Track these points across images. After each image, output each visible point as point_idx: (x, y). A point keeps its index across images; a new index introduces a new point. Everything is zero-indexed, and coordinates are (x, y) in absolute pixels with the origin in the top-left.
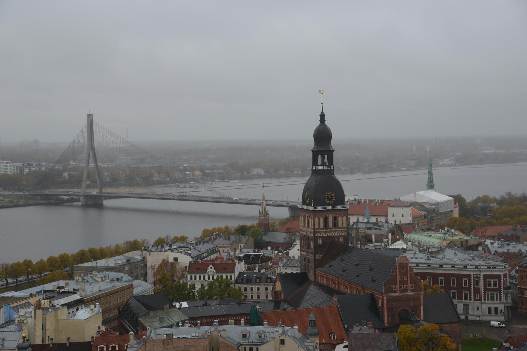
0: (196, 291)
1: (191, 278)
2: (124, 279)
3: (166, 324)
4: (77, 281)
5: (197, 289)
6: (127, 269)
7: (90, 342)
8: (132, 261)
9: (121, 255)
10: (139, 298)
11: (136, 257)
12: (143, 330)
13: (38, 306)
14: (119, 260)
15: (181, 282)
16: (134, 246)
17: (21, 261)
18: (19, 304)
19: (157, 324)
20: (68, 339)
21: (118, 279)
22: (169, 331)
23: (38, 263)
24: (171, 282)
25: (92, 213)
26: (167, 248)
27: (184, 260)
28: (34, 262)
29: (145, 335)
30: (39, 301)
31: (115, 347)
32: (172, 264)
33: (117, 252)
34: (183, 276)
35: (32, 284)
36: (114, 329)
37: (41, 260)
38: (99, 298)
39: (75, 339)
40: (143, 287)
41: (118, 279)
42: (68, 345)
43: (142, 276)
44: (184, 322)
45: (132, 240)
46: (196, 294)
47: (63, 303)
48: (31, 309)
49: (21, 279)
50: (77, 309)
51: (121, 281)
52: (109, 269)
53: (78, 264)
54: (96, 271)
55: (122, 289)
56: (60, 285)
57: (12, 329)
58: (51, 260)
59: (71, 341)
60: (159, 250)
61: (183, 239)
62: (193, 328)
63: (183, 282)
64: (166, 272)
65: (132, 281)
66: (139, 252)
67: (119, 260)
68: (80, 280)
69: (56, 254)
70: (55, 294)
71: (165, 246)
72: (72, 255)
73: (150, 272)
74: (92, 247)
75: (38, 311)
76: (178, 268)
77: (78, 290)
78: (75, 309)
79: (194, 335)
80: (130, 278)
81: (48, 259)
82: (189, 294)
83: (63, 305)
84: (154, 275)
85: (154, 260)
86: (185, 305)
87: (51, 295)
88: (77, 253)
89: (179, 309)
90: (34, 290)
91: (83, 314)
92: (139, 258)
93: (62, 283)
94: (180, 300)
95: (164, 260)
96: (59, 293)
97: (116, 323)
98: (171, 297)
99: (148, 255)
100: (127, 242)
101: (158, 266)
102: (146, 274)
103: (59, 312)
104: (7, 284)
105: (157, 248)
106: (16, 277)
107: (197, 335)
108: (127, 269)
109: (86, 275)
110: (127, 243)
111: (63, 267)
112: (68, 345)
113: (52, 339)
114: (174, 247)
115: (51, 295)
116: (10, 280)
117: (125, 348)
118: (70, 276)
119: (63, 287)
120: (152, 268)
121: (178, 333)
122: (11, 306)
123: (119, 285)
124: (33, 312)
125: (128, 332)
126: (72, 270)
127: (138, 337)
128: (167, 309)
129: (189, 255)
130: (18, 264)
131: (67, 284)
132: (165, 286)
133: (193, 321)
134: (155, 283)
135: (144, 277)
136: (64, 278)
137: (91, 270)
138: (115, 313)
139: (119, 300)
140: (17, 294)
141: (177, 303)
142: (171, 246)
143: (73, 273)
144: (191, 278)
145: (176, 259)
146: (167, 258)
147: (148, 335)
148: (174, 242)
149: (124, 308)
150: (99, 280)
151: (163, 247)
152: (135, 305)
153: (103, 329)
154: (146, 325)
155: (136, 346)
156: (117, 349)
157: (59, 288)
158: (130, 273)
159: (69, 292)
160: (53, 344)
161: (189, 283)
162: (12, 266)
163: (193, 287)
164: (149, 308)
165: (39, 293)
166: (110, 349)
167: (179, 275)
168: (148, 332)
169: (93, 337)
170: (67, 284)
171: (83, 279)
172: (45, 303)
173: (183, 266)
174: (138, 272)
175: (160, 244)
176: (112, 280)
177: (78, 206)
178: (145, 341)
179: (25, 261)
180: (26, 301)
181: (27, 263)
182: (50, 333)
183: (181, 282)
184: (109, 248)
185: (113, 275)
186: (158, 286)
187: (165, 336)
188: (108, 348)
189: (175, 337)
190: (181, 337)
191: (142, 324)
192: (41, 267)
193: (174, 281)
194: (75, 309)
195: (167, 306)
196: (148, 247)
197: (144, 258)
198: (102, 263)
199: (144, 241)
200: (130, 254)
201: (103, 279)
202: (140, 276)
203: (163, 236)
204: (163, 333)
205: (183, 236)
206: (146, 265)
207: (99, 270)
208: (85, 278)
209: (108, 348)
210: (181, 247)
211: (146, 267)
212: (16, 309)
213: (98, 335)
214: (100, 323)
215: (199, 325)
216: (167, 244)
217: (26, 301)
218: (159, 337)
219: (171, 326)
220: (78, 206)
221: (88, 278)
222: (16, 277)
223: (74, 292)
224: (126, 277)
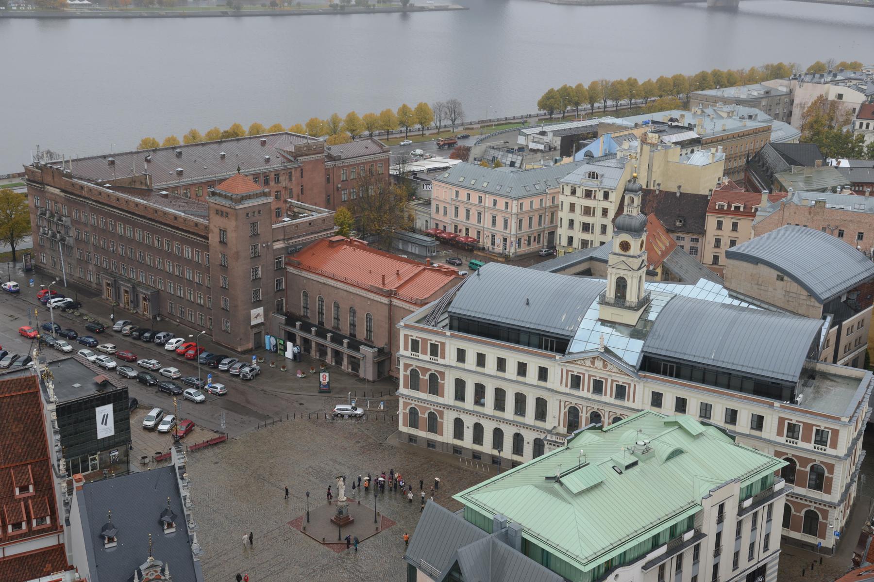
0: (866, 143)
1: (861, 126)
2: (759, 118)
3: (815, 187)
4: (695, 113)
5: (866, 143)
6: (764, 103)
7: (707, 196)
8: (773, 93)
9: (757, 82)
10: (776, 146)
11: (780, 88)
12: (780, 190)
13: (644, 141)
14: (756, 90)
15: (845, 130)
16: (777, 72)
17: (625, 79)
18: (622, 134)
19: (801, 185)
20: (679, 187)
21: (750, 117)
22: (821, 196)
23: (644, 84)
24: (826, 128)
25: (721, 18)
26: (829, 79)
27: (854, 98)
28: (640, 82)
29: (784, 197)
30: (645, 134)
31: (739, 207)
32: (833, 104)
33: (750, 79)
34: (847, 122)
35: (635, 111)
36: (738, 183)
37: (649, 80)
38: (722, 140)
39: (688, 189)
40: (785, 132)
41: (750, 117)
42: (678, 195)
43: (784, 116)
44: (843, 188)
45: (775, 63)
46: (865, 150)
47: (675, 140)
48: (636, 143)
49: (622, 102)
50: (692, 152)
51: (755, 120)
52: (739, 102)
53: (696, 90)
54: (721, 103)
55: (756, 132)
56: (674, 117)
57: (613, 165)
58: (662, 81)
59: (683, 190)
60: (815, 80)
61: (855, 67)
62: (857, 198)
63: (848, 131)
64: (821, 113)
65: (770, 121)
66: (785, 82)
67: (756, 90)
68: (699, 112)
69: (669, 74)
70: (666, 127)
71: (825, 75)
72: (689, 78)
73: (797, 112)
74: (717, 68)
75: (645, 146)
76: (842, 108)
77: (695, 126)
78: (689, 150)
79: (857, 206)
80: (767, 117)
81: (658, 80)
82: (853, 149)
83: (676, 143)
84: (804, 116)
85: (806, 94)
86: (845, 163)
87: (660, 128)
88: (696, 76)
89: (836, 167)
90: (640, 119)
91: (700, 157)
92: (784, 90)
93: (676, 114)
94: (838, 155)
95: (821, 96)
96: (671, 127)
97: (741, 176)
98: (825, 150)
99: (797, 87)
100: (768, 66)
101: (810, 104)
102: (790, 114)
103: (671, 151)
104: (605, 107)
105: (814, 77)
106: (617, 99)
107: (862, 207)
108: (764, 103)
109: (706, 107)
110: (767, 67)
111: (677, 92)
112: (678, 195)
113: (659, 185)
114: (839, 77)
115: (660, 128)
116: (609, 103)
117: (753, 210)
118: (686, 106)
119: (676, 120)
120: (802, 106)
121: (832, 201)
122: (612, 135)
123: (751, 125)
124: (639, 147)
125: (758, 191)
126: (687, 97)
127: (772, 199)
128: (818, 166)
129: (863, 91)
130: (620, 83)
131: (682, 116)
132: (818, 133)
133: (858, 188)
134: (803, 128)
135: (788, 117)
136: (677, 107)
137: (715, 100)
138: (742, 162)
139: (749, 146)
140: (619, 121)
141: (834, 160)
142: (835, 76)
143: (688, 102)
144: (861, 126)
145: (840, 96)
146: (827, 94)
147: (789, 197)
148: (842, 71)
149: (755, 157)
150: (725, 115)
151: (822, 76)
152: (772, 156)
153: (726, 181)
154: (784, 184)
155: (771, 210)
156: (742, 209)
157: (671, 120)
158: (768, 110)
159: (683, 128)
160: (660, 191)
161: (856, 133)
162: (613, 84)
163: (861, 139)
164: (792, 162)
165: (646, 123)
166: (733, 209)
167: (841, 119)
168: (790, 194)
169: (711, 190)
170: (682, 116)
171: (703, 112)
172: (653, 138)
173: (850, 107)
174: (779, 110)
175: (818, 71)
176: (742, 118)
177: (701, 9)
178: (784, 205)
179: (629, 79)
180: (630, 132)
181: (632, 83)
182: (657, 176)
183: (845, 130)
184: (741, 73)
185: (745, 111)
186: (807, 133)
187: (813, 202)
188: (729, 207)
189: (827, 206)
190: (838, 207)
191: (779, 182)
192: (647, 91)
193: (831, 127)
194: (689, 150)
195: (819, 162)
196: (800, 76)
197: (791, 91)
198: (731, 92)
199: (792, 66)
200: (771, 84)
201: (730, 115)
202: (781, 115)
203: (823, 60)
204: (812, 198)
205: (856, 63)
206: (792, 102)
207: (726, 101)
208: (705, 110)
209: (729, 207)
210: (850, 79)
211: (792, 104)
212: (619, 140)
213: (719, 189)
214: (721, 174)
215: (867, 194)
216: (830, 72)
217: (630, 132)
218: (804, 203)
219: (824, 190)
220: (701, 9)
221: (709, 111)
222: (617, 99)
223: (690, 128)
224: (762, 116)
